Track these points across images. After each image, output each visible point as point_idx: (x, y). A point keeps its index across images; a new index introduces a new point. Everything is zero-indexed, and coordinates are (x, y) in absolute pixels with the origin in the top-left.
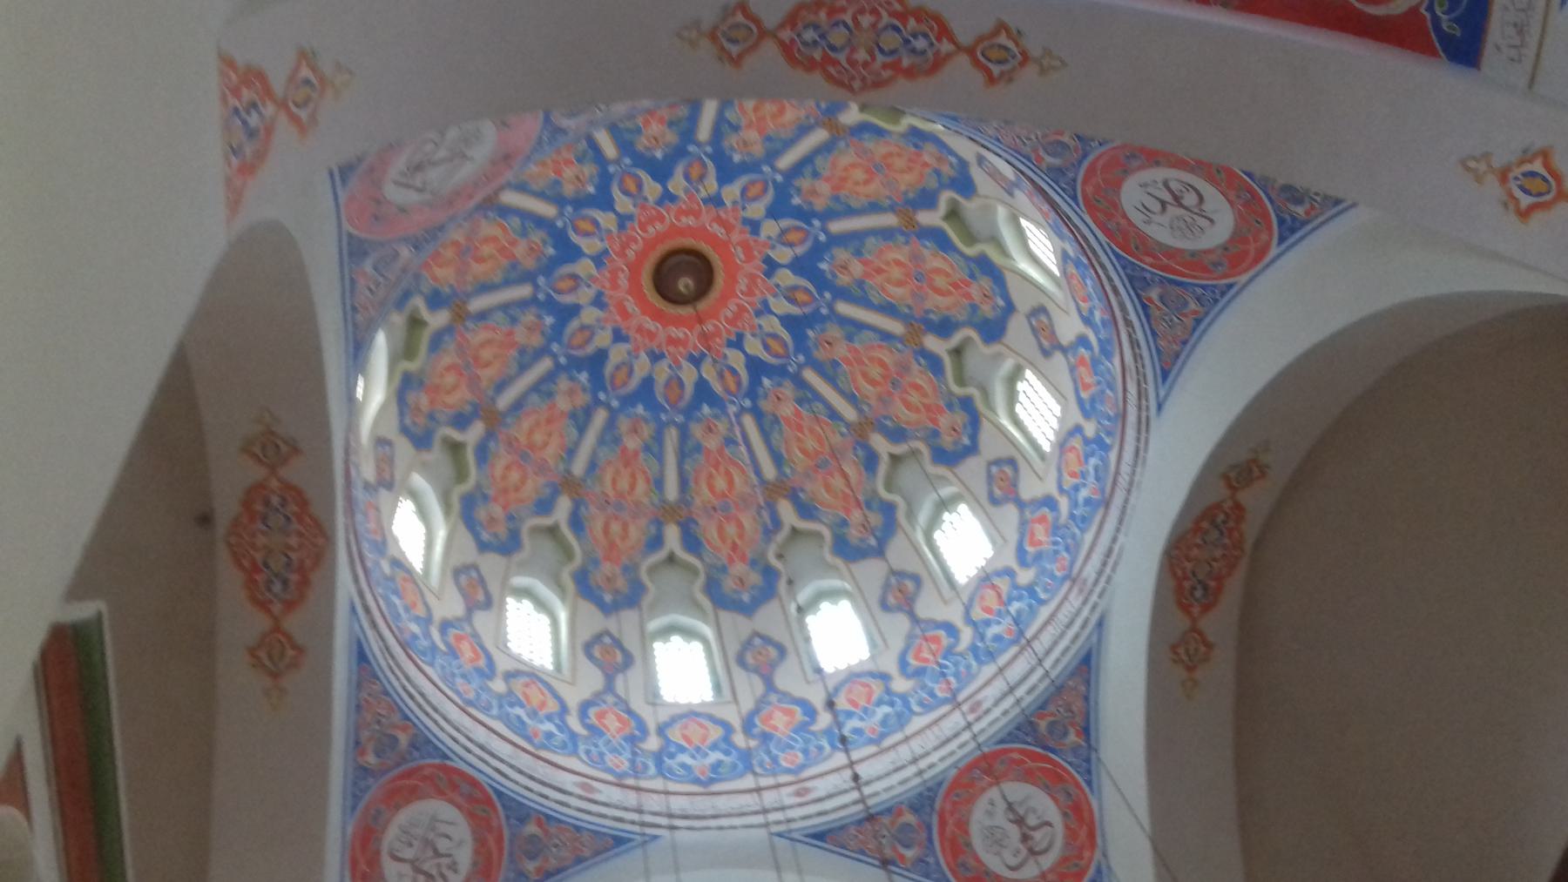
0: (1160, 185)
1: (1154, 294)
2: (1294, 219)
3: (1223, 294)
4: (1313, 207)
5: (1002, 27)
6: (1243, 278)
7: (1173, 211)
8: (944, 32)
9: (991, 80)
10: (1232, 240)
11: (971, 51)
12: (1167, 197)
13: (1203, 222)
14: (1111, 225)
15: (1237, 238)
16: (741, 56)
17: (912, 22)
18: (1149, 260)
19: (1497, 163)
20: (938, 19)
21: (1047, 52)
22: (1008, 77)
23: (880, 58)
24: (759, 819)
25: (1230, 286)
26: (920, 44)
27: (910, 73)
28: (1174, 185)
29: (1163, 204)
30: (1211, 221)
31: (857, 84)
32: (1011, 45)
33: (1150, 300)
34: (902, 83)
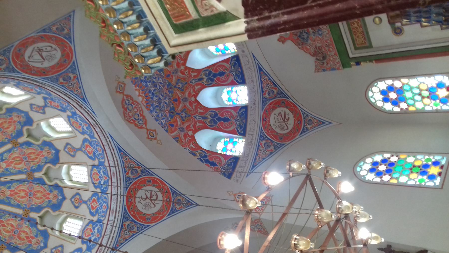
0: (150, 192)
1: (126, 224)
2: (175, 209)
3: (145, 228)
4: (182, 207)
5: (155, 131)
6: (153, 224)
7: (148, 201)
8: (146, 123)
9: (148, 138)
10: (156, 213)
11: (148, 130)
12: (149, 196)
13: (153, 206)
14: (130, 200)
15: (158, 212)
16: (119, 92)
17: (142, 117)
18: (132, 213)
19: (234, 193)
20: (146, 120)
21: (160, 140)
22: (151, 139)
23: (133, 118)
24: (117, 168)
25: (148, 226)
26: (141, 122)
27: (136, 125)
28: (153, 193)
29: (147, 198)
30: (155, 206)
31: (126, 118)
32: (155, 134)
33: (125, 225)
34: (133, 125)
